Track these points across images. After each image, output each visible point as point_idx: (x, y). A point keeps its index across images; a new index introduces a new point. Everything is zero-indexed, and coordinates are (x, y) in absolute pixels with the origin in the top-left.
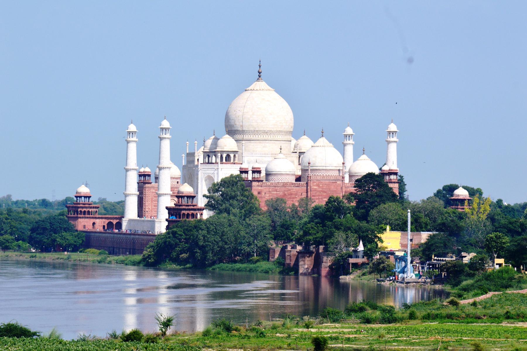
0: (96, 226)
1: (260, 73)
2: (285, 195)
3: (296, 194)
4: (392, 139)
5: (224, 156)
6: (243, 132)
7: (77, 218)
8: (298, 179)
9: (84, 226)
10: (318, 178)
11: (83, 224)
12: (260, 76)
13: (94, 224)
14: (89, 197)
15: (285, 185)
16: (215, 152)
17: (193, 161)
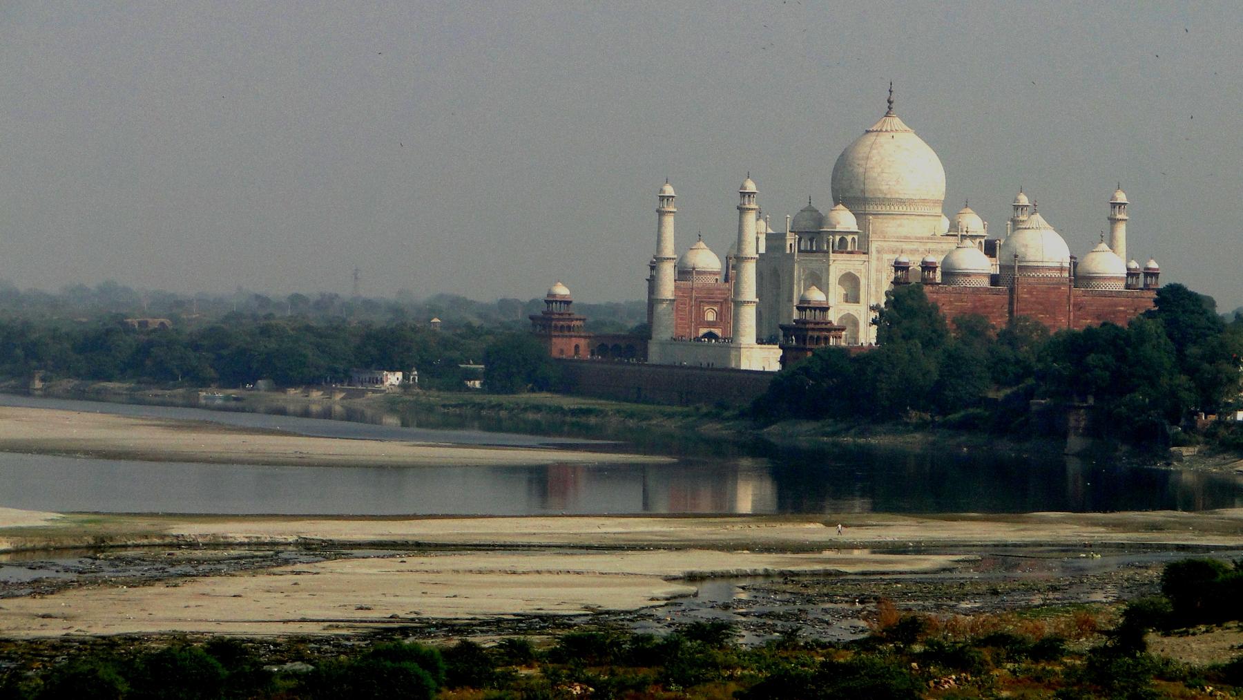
0: (582, 348)
1: (890, 102)
2: (976, 307)
3: (993, 307)
4: (1119, 217)
5: (838, 238)
6: (865, 201)
7: (551, 337)
8: (994, 280)
9: (562, 351)
10: (1030, 280)
11: (563, 347)
12: (890, 108)
13: (577, 347)
14: (568, 303)
15: (976, 291)
16: (819, 233)
17: (784, 248)
